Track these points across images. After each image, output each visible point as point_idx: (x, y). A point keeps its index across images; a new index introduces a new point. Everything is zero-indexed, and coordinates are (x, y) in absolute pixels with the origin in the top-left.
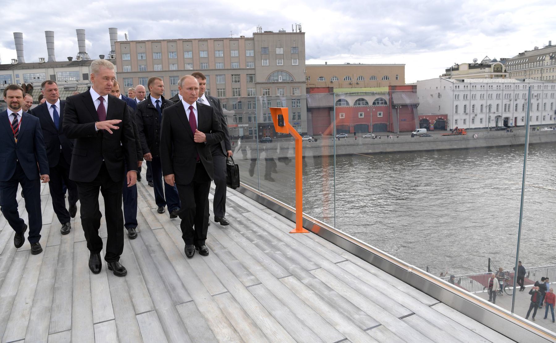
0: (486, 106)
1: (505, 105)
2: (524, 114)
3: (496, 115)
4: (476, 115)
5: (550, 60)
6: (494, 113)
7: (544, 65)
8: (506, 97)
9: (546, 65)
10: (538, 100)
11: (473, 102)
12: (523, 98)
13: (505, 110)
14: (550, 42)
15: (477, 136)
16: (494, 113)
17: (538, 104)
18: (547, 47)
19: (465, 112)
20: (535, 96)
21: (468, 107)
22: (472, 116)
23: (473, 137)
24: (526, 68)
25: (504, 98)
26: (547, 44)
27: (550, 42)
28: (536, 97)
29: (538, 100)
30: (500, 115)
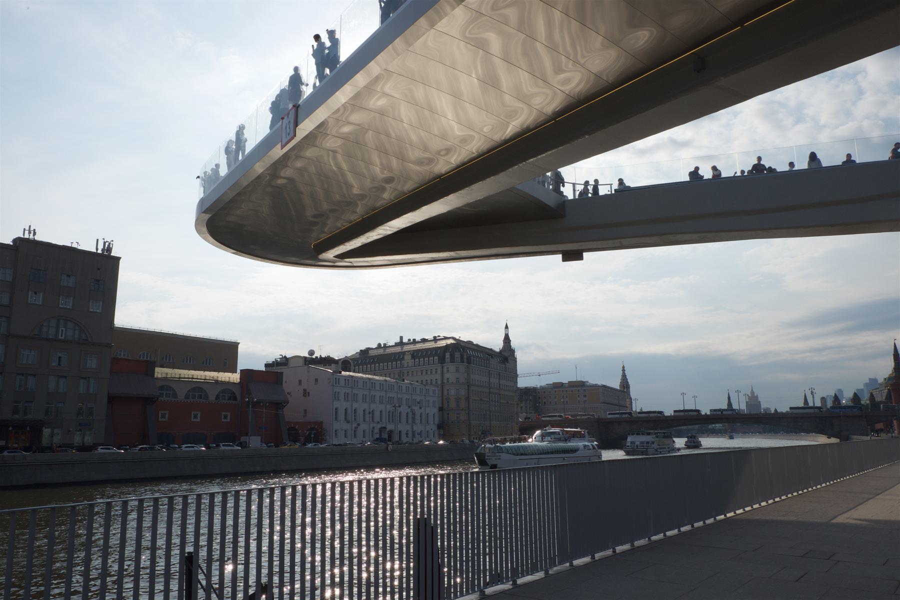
0: (370, 413)
1: (389, 412)
2: (409, 427)
3: (379, 426)
4: (359, 425)
5: (411, 359)
6: (378, 423)
7: (403, 366)
8: (389, 402)
9: (406, 366)
10: (421, 408)
11: (355, 405)
12: (406, 405)
13: (389, 421)
14: (401, 338)
15: (391, 447)
16: (378, 423)
17: (421, 414)
18: (397, 345)
19: (346, 419)
20: (418, 403)
21: (349, 411)
22: (355, 425)
23: (387, 449)
24: (375, 371)
25: (387, 402)
26: (398, 340)
27: (401, 338)
28: (419, 405)
29: (421, 408)
30: (384, 426)
